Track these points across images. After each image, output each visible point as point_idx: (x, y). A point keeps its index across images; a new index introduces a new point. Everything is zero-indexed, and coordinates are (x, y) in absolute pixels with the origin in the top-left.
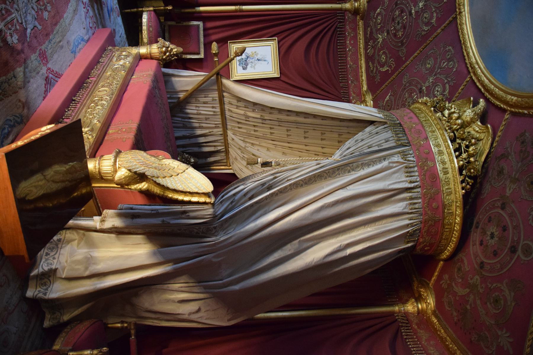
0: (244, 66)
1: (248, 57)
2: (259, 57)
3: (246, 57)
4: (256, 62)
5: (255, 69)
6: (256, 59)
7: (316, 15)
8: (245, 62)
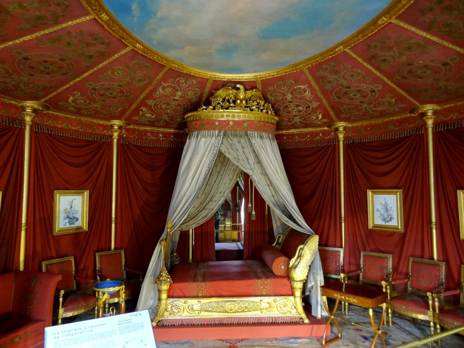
0: (75, 220)
1: (68, 217)
2: (68, 207)
3: (68, 219)
4: (73, 209)
5: (78, 211)
6: (70, 209)
8: (72, 219)
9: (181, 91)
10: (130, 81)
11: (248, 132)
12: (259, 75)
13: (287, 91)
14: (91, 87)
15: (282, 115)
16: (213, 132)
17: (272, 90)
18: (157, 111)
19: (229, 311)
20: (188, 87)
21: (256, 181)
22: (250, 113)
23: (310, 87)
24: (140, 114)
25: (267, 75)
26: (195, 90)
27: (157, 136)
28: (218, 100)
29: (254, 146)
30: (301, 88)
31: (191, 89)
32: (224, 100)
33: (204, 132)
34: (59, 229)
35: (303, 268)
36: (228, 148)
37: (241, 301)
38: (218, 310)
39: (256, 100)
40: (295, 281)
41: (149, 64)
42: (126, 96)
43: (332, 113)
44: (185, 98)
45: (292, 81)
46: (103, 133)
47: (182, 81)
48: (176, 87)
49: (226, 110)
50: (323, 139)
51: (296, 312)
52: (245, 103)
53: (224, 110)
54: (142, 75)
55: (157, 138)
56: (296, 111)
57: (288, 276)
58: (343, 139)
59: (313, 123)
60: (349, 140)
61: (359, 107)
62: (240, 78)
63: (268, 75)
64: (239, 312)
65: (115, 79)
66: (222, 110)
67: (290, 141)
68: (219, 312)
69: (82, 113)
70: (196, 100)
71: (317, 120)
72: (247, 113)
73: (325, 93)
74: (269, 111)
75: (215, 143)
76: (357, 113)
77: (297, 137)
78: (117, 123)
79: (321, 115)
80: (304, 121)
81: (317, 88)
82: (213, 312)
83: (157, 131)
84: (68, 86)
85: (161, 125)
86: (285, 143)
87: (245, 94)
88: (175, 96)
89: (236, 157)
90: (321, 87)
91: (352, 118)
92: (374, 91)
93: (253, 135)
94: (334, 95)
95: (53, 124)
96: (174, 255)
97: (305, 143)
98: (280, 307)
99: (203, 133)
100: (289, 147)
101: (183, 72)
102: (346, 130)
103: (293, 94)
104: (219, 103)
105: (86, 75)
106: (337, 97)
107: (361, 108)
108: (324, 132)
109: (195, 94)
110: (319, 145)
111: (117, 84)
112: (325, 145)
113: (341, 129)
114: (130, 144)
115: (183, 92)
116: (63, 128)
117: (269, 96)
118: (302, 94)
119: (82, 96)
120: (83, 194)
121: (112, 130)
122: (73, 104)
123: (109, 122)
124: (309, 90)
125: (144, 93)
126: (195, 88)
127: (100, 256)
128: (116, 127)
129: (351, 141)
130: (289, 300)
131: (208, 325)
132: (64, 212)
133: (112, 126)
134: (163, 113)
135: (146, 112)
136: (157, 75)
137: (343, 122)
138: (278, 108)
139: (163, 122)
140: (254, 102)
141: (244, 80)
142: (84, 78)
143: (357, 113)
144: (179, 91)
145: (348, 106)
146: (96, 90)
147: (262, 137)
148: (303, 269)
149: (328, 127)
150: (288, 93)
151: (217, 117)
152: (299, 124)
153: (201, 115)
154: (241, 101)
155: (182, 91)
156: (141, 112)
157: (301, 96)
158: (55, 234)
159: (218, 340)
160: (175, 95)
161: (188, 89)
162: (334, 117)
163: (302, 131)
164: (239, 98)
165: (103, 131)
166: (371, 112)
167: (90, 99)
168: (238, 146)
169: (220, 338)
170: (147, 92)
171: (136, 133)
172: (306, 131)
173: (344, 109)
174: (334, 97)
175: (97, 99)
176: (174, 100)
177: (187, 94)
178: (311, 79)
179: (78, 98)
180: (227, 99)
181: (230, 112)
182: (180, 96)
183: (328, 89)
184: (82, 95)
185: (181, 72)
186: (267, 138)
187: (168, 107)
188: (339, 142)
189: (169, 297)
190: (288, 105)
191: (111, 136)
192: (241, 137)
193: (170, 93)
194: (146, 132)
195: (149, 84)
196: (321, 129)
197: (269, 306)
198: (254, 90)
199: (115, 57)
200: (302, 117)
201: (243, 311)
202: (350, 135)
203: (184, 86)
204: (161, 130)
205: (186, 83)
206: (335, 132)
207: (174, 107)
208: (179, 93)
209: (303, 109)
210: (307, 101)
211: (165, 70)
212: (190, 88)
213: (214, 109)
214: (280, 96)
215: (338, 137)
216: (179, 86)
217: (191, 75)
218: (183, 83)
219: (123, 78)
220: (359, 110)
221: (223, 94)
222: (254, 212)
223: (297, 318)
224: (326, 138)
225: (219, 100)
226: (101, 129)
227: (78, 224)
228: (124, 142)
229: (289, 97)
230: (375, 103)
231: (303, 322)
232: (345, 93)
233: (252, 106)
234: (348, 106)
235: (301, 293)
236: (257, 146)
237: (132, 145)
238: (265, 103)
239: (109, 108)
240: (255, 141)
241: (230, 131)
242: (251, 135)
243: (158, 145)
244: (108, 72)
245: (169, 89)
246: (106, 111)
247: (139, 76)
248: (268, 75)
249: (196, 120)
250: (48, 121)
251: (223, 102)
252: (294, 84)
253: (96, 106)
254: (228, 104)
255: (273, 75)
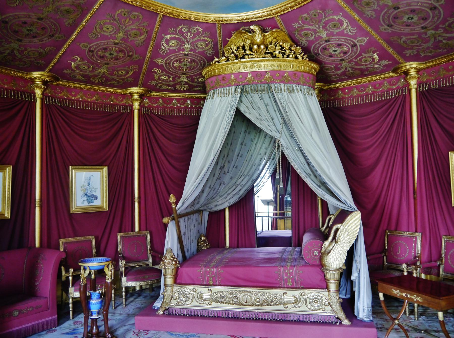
1: (86, 195)
2: (86, 184)
3: (86, 196)
4: (91, 186)
5: (97, 188)
6: (88, 187)
7: (48, 127)
9: (188, 43)
10: (126, 37)
11: (273, 86)
12: (275, 9)
13: (317, 26)
14: (87, 49)
15: (324, 60)
16: (229, 89)
17: (298, 27)
18: (171, 71)
19: (244, 303)
20: (194, 37)
21: (283, 146)
22: (273, 60)
23: (346, 16)
24: (155, 77)
25: (283, 8)
26: (204, 40)
27: (184, 103)
28: (232, 49)
29: (280, 101)
30: (333, 20)
31: (199, 38)
32: (238, 48)
33: (220, 89)
34: (76, 207)
35: (338, 253)
36: (249, 107)
37: (259, 292)
38: (231, 301)
39: (279, 43)
40: (327, 270)
41: (137, 13)
42: (128, 56)
43: (391, 50)
44: (197, 51)
45: (318, 11)
46: (122, 103)
47: (185, 30)
48: (181, 39)
49: (242, 60)
50: (390, 89)
51: (331, 310)
52: (264, 49)
53: (239, 60)
54: (135, 27)
55: (185, 105)
56: (340, 53)
57: (321, 265)
58: (416, 86)
59: (370, 68)
60: (423, 86)
61: (423, 36)
62: (252, 16)
63: (285, 7)
64: (256, 305)
65: (107, 36)
66: (237, 61)
67: (347, 96)
68: (234, 304)
69: (93, 81)
70: (212, 53)
71: (373, 63)
72: (269, 60)
73: (369, 21)
74: (298, 56)
75: (231, 101)
76: (425, 46)
77: (355, 91)
78: (135, 90)
79: (376, 54)
80: (356, 67)
81: (356, 16)
82: (225, 303)
83: (183, 97)
84: (63, 50)
85: (184, 89)
86: (340, 99)
87: (264, 37)
88: (184, 50)
89: (259, 117)
90: (361, 14)
91: (422, 55)
92: (435, 8)
93: (278, 89)
94: (383, 24)
95: (66, 96)
96: (201, 240)
97: (366, 97)
98: (310, 303)
99: (219, 91)
100: (345, 104)
101: (181, 18)
102: (419, 73)
103: (327, 30)
104: (233, 52)
105: (75, 34)
106: (388, 26)
107: (427, 36)
108: (390, 80)
109: (207, 45)
110: (384, 98)
111: (112, 42)
112: (392, 97)
113: (413, 73)
114: (153, 114)
115: (191, 44)
116: (77, 100)
117: (298, 37)
118: (339, 28)
119: (83, 61)
120: (101, 171)
121: (132, 99)
122: (78, 71)
123: (126, 90)
124: (347, 21)
125: (148, 51)
126: (204, 37)
127: (122, 237)
128: (136, 96)
129: (426, 87)
130: (321, 294)
131: (219, 318)
132: (81, 189)
133: (131, 95)
134: (180, 73)
135: (161, 74)
136: (154, 27)
137: (412, 63)
138: (316, 51)
139: (184, 84)
140: (276, 46)
141: (259, 19)
142: (75, 40)
143: (425, 46)
144: (186, 43)
145: (409, 37)
146: (93, 51)
147: (290, 91)
148: (339, 255)
149: (394, 71)
150: (319, 28)
151: (232, 69)
152: (352, 71)
153: (216, 69)
154: (259, 46)
155: (190, 43)
156: (155, 75)
157: (338, 30)
158: (72, 212)
159: (230, 336)
160: (183, 48)
161: (195, 40)
162: (396, 56)
163: (360, 82)
164: (255, 42)
165: (122, 101)
166: (444, 41)
167: (93, 64)
168: (260, 104)
169: (232, 335)
170: (150, 48)
171: (160, 101)
172: (366, 82)
173: (404, 42)
174: (384, 26)
175: (99, 62)
176: (185, 55)
177: (197, 45)
178: (343, 4)
179: (80, 63)
180: (241, 46)
181: (248, 62)
182: (189, 49)
183: (372, 16)
184: (82, 59)
185: (178, 19)
186: (298, 91)
187: (182, 65)
188: (410, 90)
189: (176, 282)
190: (327, 46)
191: (131, 106)
192: (262, 91)
193: (177, 47)
194: (171, 99)
195: (148, 39)
196: (386, 76)
197: (295, 300)
198: (274, 30)
199: (95, 9)
200: (351, 61)
201: (262, 305)
202: (425, 80)
203: (189, 36)
204: (188, 95)
205: (191, 33)
206: (404, 79)
207: (189, 65)
208: (187, 46)
209: (349, 49)
210: (349, 37)
211: (160, 19)
212: (197, 38)
213: (228, 60)
214: (312, 34)
215: (408, 85)
216: (184, 37)
217: (192, 20)
218: (187, 33)
219: (115, 33)
220: (426, 41)
221: (238, 41)
222: (283, 184)
223: (332, 317)
224: (394, 87)
225: (232, 48)
226: (119, 98)
227: (97, 203)
228: (146, 112)
229: (324, 35)
230: (444, 26)
231: (341, 323)
232: (396, 17)
233: (274, 51)
234: (409, 37)
235: (337, 285)
236: (284, 102)
237: (155, 115)
238: (291, 46)
239: (117, 73)
240: (282, 95)
241: (250, 86)
242: (277, 89)
243: (186, 114)
244: (96, 29)
245: (173, 42)
246: (116, 76)
247: (132, 29)
248: (285, 7)
249: (211, 77)
250: (60, 93)
251: (236, 50)
252: (323, 14)
253: (102, 72)
254: (243, 51)
255: (291, 7)
